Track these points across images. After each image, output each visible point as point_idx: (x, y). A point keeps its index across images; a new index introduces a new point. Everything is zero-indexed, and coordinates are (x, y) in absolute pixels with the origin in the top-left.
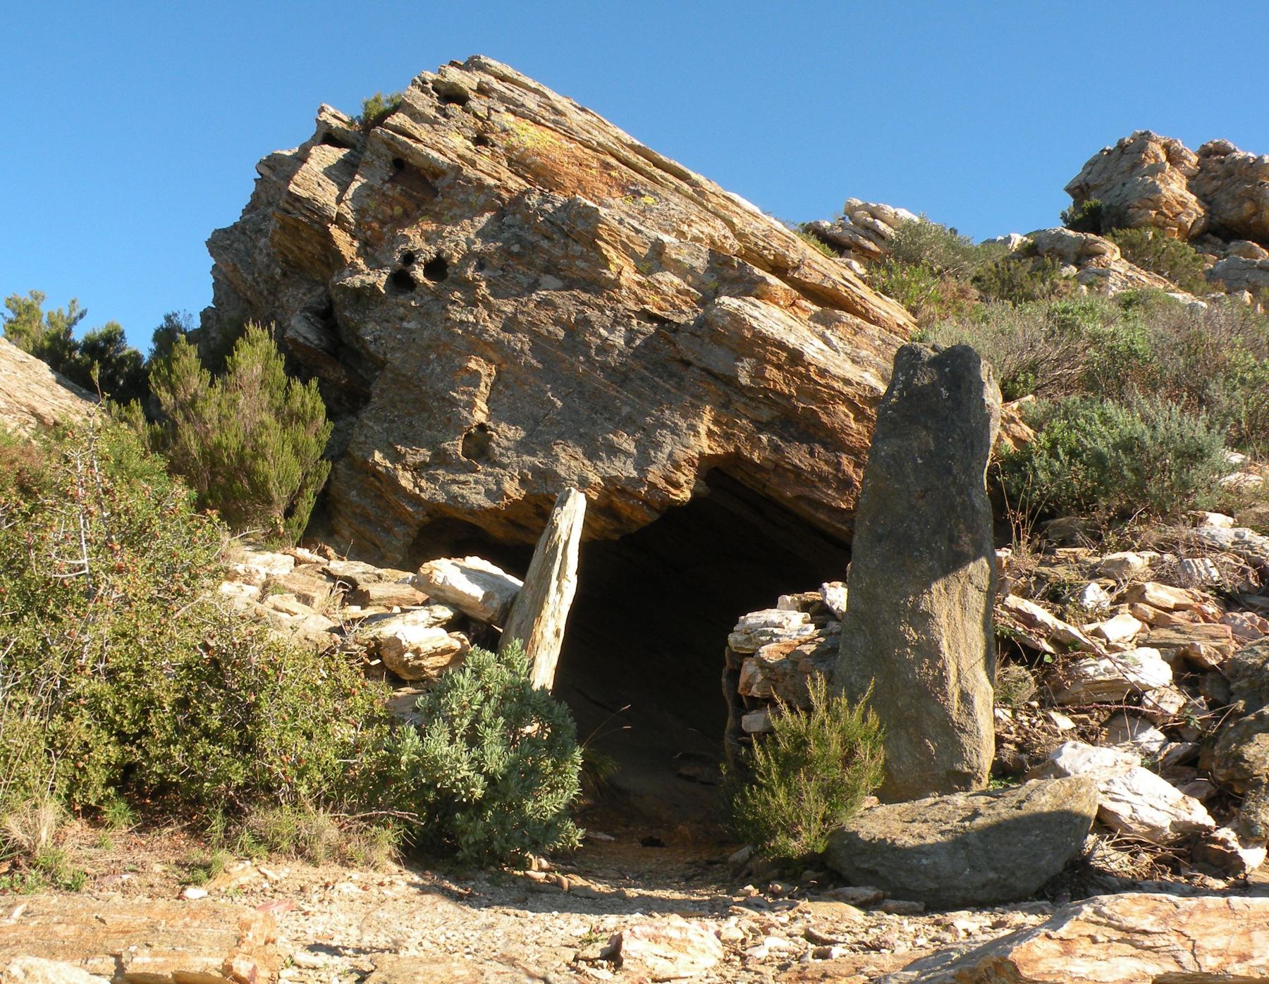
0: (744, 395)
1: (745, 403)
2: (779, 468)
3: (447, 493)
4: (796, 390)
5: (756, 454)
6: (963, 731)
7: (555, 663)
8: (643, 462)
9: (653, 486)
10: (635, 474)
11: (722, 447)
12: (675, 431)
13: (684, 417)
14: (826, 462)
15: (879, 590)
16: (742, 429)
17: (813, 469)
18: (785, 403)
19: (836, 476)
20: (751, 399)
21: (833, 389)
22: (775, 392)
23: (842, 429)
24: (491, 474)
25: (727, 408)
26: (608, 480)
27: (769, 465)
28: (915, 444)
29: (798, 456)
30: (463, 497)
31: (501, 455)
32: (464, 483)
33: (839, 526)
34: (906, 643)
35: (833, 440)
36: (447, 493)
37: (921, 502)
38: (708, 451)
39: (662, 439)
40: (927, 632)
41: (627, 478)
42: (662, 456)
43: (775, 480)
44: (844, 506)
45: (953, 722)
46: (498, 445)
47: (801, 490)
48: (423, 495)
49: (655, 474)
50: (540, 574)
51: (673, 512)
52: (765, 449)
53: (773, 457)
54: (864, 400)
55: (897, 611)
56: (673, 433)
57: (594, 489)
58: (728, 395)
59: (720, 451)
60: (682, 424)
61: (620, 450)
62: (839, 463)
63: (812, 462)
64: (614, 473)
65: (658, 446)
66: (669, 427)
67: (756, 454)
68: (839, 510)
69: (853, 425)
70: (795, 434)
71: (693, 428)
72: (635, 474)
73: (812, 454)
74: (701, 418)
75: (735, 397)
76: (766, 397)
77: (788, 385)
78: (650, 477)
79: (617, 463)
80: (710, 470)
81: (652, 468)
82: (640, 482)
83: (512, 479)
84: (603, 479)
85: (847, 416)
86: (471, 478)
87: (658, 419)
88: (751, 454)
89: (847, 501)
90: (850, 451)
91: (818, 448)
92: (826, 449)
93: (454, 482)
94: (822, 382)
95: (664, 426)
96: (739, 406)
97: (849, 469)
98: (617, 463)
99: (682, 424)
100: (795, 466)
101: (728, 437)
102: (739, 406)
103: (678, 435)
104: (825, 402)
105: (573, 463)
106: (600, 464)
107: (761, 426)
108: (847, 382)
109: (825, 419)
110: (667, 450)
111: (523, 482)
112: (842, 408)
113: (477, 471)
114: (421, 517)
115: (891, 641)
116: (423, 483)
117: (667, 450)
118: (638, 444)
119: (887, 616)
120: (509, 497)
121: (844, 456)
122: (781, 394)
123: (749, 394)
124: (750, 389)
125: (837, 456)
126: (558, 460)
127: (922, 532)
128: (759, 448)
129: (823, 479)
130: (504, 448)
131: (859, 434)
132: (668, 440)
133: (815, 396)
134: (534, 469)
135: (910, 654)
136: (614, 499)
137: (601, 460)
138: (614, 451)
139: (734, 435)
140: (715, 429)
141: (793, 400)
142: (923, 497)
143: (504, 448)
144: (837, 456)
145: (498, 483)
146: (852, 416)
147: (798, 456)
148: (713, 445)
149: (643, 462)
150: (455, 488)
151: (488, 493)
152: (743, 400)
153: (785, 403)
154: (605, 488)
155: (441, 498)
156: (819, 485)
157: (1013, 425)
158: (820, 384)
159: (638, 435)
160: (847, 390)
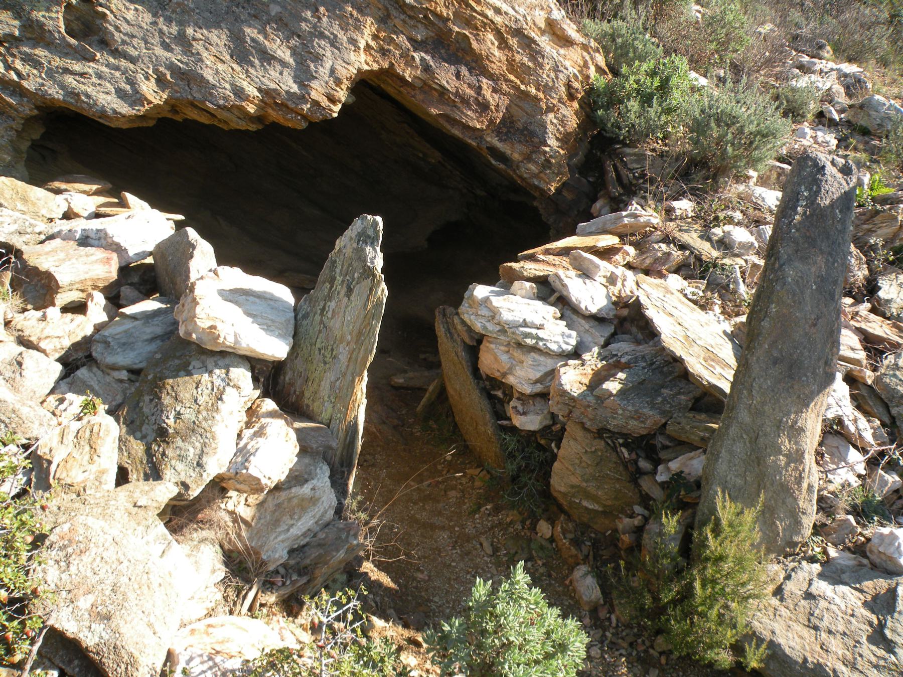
0: (405, 13)
1: (404, 21)
2: (428, 86)
3: (62, 86)
4: (454, 14)
5: (408, 72)
6: (804, 513)
7: (146, 205)
8: (304, 77)
9: (316, 103)
10: (295, 88)
11: (378, 62)
12: (334, 43)
13: (344, 28)
14: (470, 86)
15: (766, 408)
16: (398, 46)
17: (457, 91)
18: (441, 25)
19: (476, 99)
20: (410, 17)
21: (486, 17)
22: (434, 13)
23: (487, 56)
24: (117, 68)
25: (385, 23)
26: (266, 92)
27: (418, 84)
28: (813, 269)
29: (446, 77)
30: (88, 96)
31: (124, 42)
32: (82, 75)
33: (470, 141)
34: (780, 452)
35: (477, 64)
36: (62, 86)
37: (813, 330)
38: (366, 68)
39: (321, 51)
40: (796, 443)
41: (287, 92)
42: (324, 71)
43: (420, 97)
44: (478, 127)
45: (799, 508)
46: (117, 28)
47: (448, 110)
48: (25, 84)
49: (317, 91)
50: (360, 333)
51: (329, 123)
52: (417, 67)
53: (424, 76)
54: (509, 30)
55: (779, 426)
56: (332, 45)
57: (252, 102)
58: (387, 9)
59: (375, 67)
60: (342, 37)
61: (274, 58)
62: (480, 88)
63: (457, 84)
64: (273, 86)
65: (318, 59)
66: (328, 38)
67: (408, 72)
68: (474, 129)
69: (497, 53)
70: (444, 55)
71: (353, 42)
72: (295, 88)
73: (458, 76)
74: (362, 34)
75: (394, 12)
76: (426, 17)
77: (447, 7)
78: (314, 95)
79: (272, 73)
80: (363, 85)
81: (315, 84)
82: (303, 98)
83: (147, 78)
84: (260, 90)
85: (493, 44)
86: (90, 68)
87: (315, 27)
88: (404, 71)
89: (482, 122)
90: (491, 77)
91: (464, 71)
92: (470, 73)
93: (67, 71)
94: (478, 9)
95: (322, 36)
96: (398, 22)
97: (487, 93)
98: (272, 73)
99: (341, 35)
100: (443, 87)
101: (384, 52)
102: (398, 22)
103: (338, 49)
104: (477, 29)
105: (221, 67)
106: (251, 70)
107: (418, 45)
108: (498, 11)
109: (475, 45)
110: (328, 65)
111: (161, 81)
112: (490, 36)
113: (93, 59)
114: (27, 110)
115: (768, 450)
116: (18, 65)
117: (328, 65)
118: (294, 52)
119: (768, 430)
120: (150, 102)
121: (485, 80)
122: (439, 16)
123: (409, 13)
124: (412, 7)
125: (478, 81)
126: (201, 60)
127: (810, 358)
128: (412, 66)
129: (465, 101)
130: (126, 34)
131: (500, 61)
132: (328, 54)
133: (468, 22)
134: (171, 67)
135: (782, 460)
136: (270, 111)
137: (253, 66)
138: (267, 58)
139: (389, 51)
140: (373, 44)
141: (450, 24)
142: (815, 325)
143: (126, 34)
144: (478, 81)
145: (132, 82)
146: (496, 43)
147: (446, 77)
148: (369, 59)
149: (304, 77)
150: (70, 80)
151: (121, 94)
152: (403, 17)
153: (441, 25)
154: (262, 101)
155: (55, 92)
156: (460, 105)
157: (597, 55)
158: (475, 11)
159: (293, 42)
160: (498, 19)
